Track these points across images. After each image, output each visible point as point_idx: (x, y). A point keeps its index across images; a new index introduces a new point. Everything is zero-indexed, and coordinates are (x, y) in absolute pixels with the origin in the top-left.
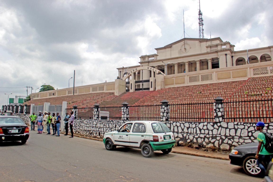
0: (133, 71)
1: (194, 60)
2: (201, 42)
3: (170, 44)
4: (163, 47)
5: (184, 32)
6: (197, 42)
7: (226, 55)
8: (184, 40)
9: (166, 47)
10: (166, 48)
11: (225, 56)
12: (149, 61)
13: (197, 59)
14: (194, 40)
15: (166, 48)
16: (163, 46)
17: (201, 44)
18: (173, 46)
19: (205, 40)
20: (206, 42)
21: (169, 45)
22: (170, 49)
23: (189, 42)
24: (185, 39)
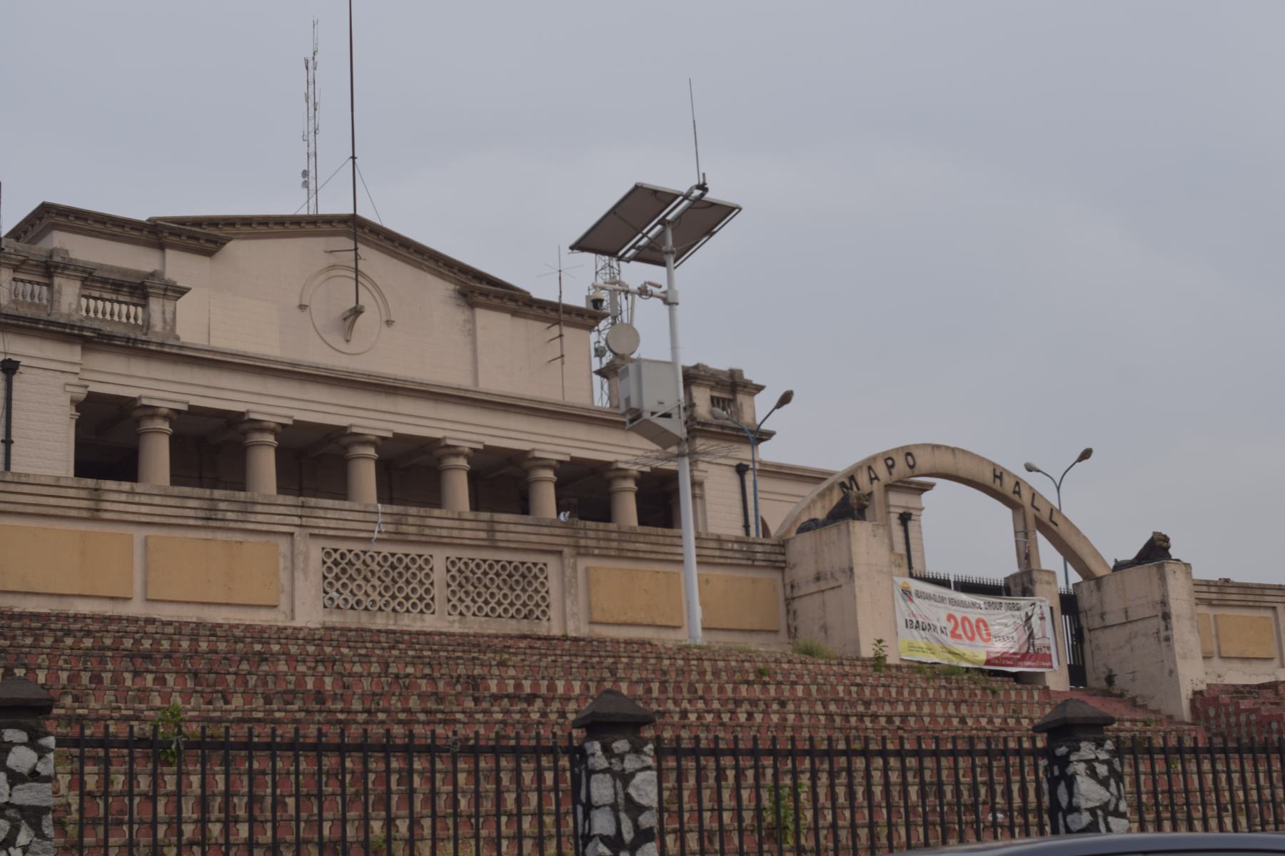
0: (890, 468)
1: (525, 446)
2: (472, 305)
3: (214, 222)
4: (142, 215)
5: (353, 158)
6: (441, 289)
7: (741, 470)
8: (341, 227)
9: (173, 233)
10: (161, 247)
11: (734, 480)
12: (107, 329)
13: (556, 443)
14: (418, 266)
15: (174, 239)
16: (141, 214)
17: (473, 321)
18: (238, 249)
19: (513, 299)
20: (515, 313)
21: (198, 222)
22: (207, 259)
23: (374, 261)
24: (356, 228)
